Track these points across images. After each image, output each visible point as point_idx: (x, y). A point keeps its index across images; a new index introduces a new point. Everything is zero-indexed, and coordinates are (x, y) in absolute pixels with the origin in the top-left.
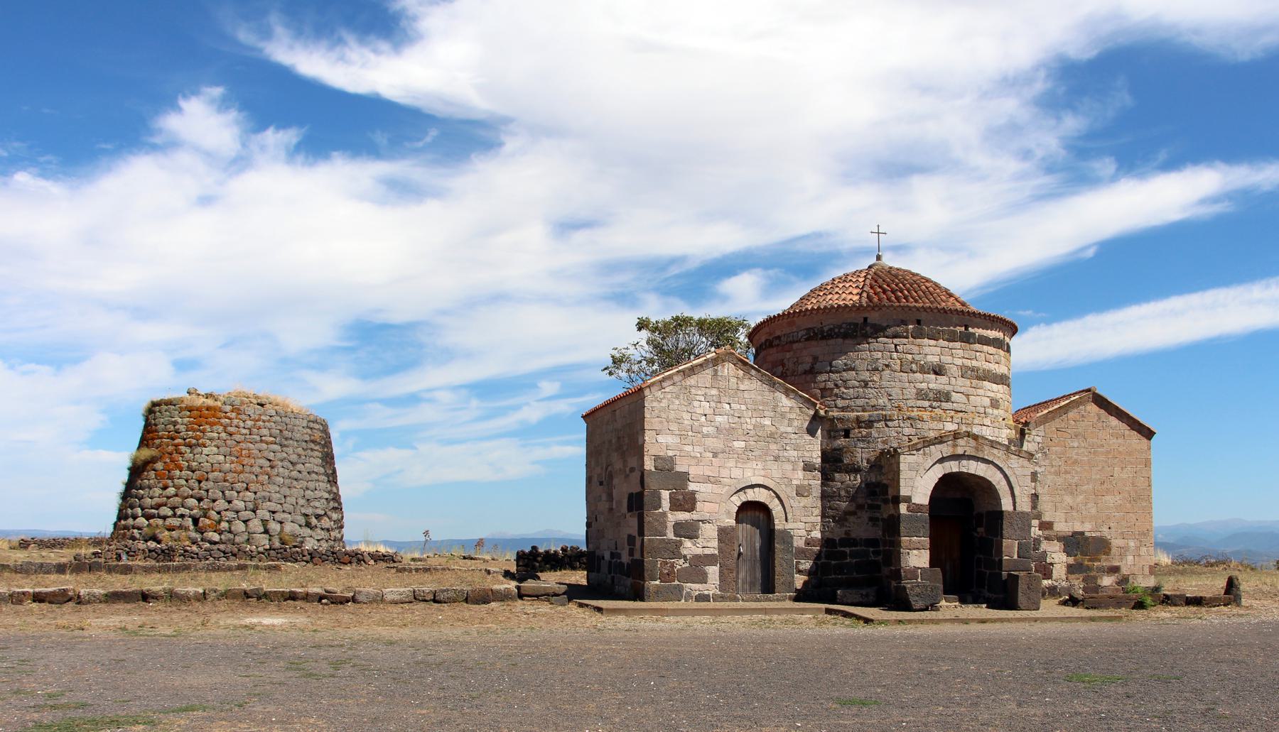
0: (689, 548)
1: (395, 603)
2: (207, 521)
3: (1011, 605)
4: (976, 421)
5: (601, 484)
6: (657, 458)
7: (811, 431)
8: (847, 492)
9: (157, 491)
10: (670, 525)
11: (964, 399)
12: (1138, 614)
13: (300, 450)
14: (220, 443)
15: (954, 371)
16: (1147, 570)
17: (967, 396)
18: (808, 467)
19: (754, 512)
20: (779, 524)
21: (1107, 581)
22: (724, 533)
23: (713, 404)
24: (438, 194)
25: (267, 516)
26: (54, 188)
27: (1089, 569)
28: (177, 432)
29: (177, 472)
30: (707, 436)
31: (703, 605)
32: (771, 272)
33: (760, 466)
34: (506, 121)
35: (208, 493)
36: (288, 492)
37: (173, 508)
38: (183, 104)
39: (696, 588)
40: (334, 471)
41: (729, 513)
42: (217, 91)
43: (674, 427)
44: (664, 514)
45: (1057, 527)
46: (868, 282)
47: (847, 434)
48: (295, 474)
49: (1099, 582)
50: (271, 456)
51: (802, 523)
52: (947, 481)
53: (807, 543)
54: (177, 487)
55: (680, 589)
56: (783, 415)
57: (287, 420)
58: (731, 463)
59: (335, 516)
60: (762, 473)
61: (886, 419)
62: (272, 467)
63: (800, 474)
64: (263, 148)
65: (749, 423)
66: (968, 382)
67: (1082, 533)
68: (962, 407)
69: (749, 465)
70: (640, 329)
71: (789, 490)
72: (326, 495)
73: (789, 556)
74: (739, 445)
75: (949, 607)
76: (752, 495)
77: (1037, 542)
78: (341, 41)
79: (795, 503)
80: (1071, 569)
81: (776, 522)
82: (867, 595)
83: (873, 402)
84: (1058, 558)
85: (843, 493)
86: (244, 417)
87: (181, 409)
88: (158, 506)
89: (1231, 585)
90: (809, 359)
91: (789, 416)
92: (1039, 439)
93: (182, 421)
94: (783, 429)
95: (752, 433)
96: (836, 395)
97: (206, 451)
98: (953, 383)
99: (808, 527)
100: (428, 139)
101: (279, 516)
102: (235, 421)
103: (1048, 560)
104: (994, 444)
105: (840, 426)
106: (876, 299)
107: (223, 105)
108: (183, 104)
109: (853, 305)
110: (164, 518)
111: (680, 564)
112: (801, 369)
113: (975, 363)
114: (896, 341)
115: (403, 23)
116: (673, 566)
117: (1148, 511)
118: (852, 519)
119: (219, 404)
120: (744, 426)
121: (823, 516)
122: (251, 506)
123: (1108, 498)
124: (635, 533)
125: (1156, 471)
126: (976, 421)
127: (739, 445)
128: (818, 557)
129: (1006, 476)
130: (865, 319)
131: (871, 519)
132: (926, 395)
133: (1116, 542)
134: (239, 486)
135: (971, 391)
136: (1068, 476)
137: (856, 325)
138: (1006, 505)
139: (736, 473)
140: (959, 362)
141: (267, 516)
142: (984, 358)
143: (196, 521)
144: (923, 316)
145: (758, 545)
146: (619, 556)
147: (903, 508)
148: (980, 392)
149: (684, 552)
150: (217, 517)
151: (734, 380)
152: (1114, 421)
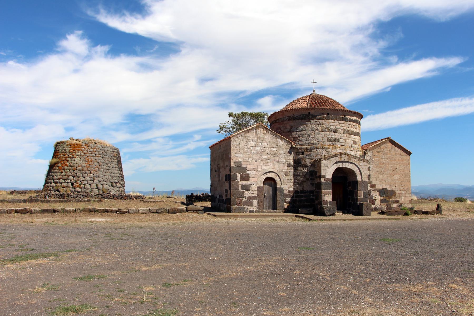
0: (247, 194)
1: (143, 213)
2: (77, 184)
3: (360, 214)
4: (348, 149)
5: (216, 171)
6: (235, 162)
8: (303, 174)
9: (59, 174)
10: (240, 186)
11: (344, 141)
12: (406, 217)
13: (109, 159)
14: (81, 157)
16: (409, 202)
17: (345, 140)
18: (289, 165)
19: (270, 181)
20: (279, 185)
21: (395, 206)
22: (259, 189)
23: (255, 143)
24: (158, 68)
25: (98, 183)
26: (22, 67)
27: (388, 201)
28: (66, 153)
29: (66, 167)
30: (253, 154)
31: (252, 214)
32: (276, 96)
33: (272, 165)
34: (182, 43)
35: (77, 174)
36: (105, 174)
37: (65, 180)
38: (68, 37)
39: (249, 208)
40: (121, 167)
41: (261, 181)
42: (80, 32)
43: (242, 151)
44: (238, 182)
45: (377, 187)
46: (310, 100)
47: (303, 154)
48: (107, 168)
49: (392, 206)
50: (99, 161)
51: (287, 185)
52: (338, 171)
53: (289, 192)
54: (66, 172)
55: (244, 208)
56: (280, 147)
57: (105, 149)
58: (262, 164)
59: (122, 183)
60: (273, 167)
61: (317, 148)
62: (99, 165)
63: (286, 168)
64: (96, 52)
65: (268, 150)
66: (345, 135)
67: (386, 189)
69: (268, 164)
70: (229, 116)
71: (282, 173)
72: (119, 175)
74: (264, 157)
75: (339, 215)
76: (269, 175)
77: (370, 192)
78: (124, 15)
79: (284, 178)
80: (382, 201)
81: (278, 185)
82: (310, 211)
83: (312, 142)
84: (377, 197)
85: (301, 174)
86: (89, 147)
87: (67, 145)
88: (59, 179)
89: (438, 207)
90: (289, 127)
91: (282, 147)
92: (370, 155)
93: (68, 149)
94: (280, 152)
95: (269, 153)
96: (299, 140)
97: (76, 159)
98: (341, 135)
99: (289, 186)
100: (155, 49)
101: (102, 183)
102: (87, 149)
104: (354, 157)
105: (300, 151)
106: (313, 106)
107: (82, 37)
108: (68, 37)
109: (305, 108)
110: (61, 183)
112: (286, 130)
113: (348, 128)
114: (320, 121)
115: (146, 8)
116: (241, 200)
117: (409, 181)
118: (304, 183)
119: (81, 143)
121: (294, 182)
122: (92, 179)
123: (395, 176)
124: (228, 189)
125: (412, 167)
126: (348, 149)
127: (264, 157)
128: (292, 197)
130: (309, 113)
131: (311, 184)
132: (331, 140)
133: (398, 192)
134: (88, 172)
135: (347, 138)
136: (381, 168)
138: (359, 179)
139: (264, 167)
140: (342, 128)
141: (98, 183)
142: (351, 127)
143: (72, 184)
144: (330, 112)
145: (271, 193)
146: (222, 197)
147: (322, 180)
148: (350, 139)
149: (245, 195)
150: (80, 183)
151: (263, 135)
152: (397, 149)
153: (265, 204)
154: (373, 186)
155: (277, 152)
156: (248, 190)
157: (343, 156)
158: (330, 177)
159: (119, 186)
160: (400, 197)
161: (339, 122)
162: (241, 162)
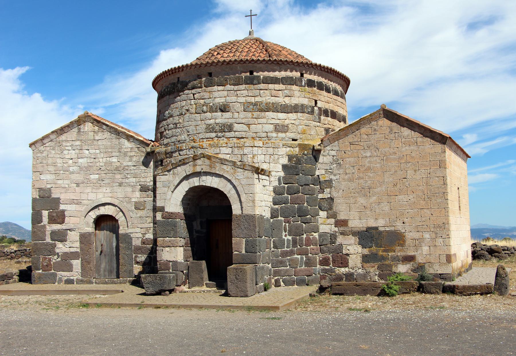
0: (61, 248)
7: (146, 164)
10: (48, 234)
11: (245, 128)
15: (239, 107)
18: (144, 189)
20: (122, 230)
22: (84, 238)
23: (77, 151)
27: (383, 258)
30: (73, 173)
31: (70, 287)
39: (64, 275)
43: (51, 169)
44: (44, 226)
45: (351, 224)
53: (143, 243)
55: (55, 275)
56: (125, 154)
60: (110, 195)
63: (138, 194)
65: (102, 161)
66: (249, 115)
67: (376, 228)
68: (244, 134)
69: (100, 190)
71: (129, 206)
73: (129, 252)
80: (365, 259)
81: (121, 228)
83: (179, 138)
84: (354, 250)
91: (129, 154)
92: (333, 153)
94: (125, 164)
95: (103, 168)
98: (237, 117)
99: (143, 231)
103: (344, 252)
104: (223, 162)
111: (55, 259)
113: (258, 99)
114: (194, 91)
116: (50, 260)
120: (98, 164)
123: (400, 197)
129: (234, 187)
133: (410, 235)
136: (361, 181)
137: (174, 84)
138: (236, 210)
139: (92, 196)
140: (242, 100)
144: (212, 69)
149: (57, 251)
151: (92, 134)
152: (406, 131)
153: (103, 266)
154: (341, 223)
155: (118, 164)
156: (63, 239)
157: (199, 162)
158: (180, 210)
160: (417, 247)
161: (236, 88)
162: (50, 189)
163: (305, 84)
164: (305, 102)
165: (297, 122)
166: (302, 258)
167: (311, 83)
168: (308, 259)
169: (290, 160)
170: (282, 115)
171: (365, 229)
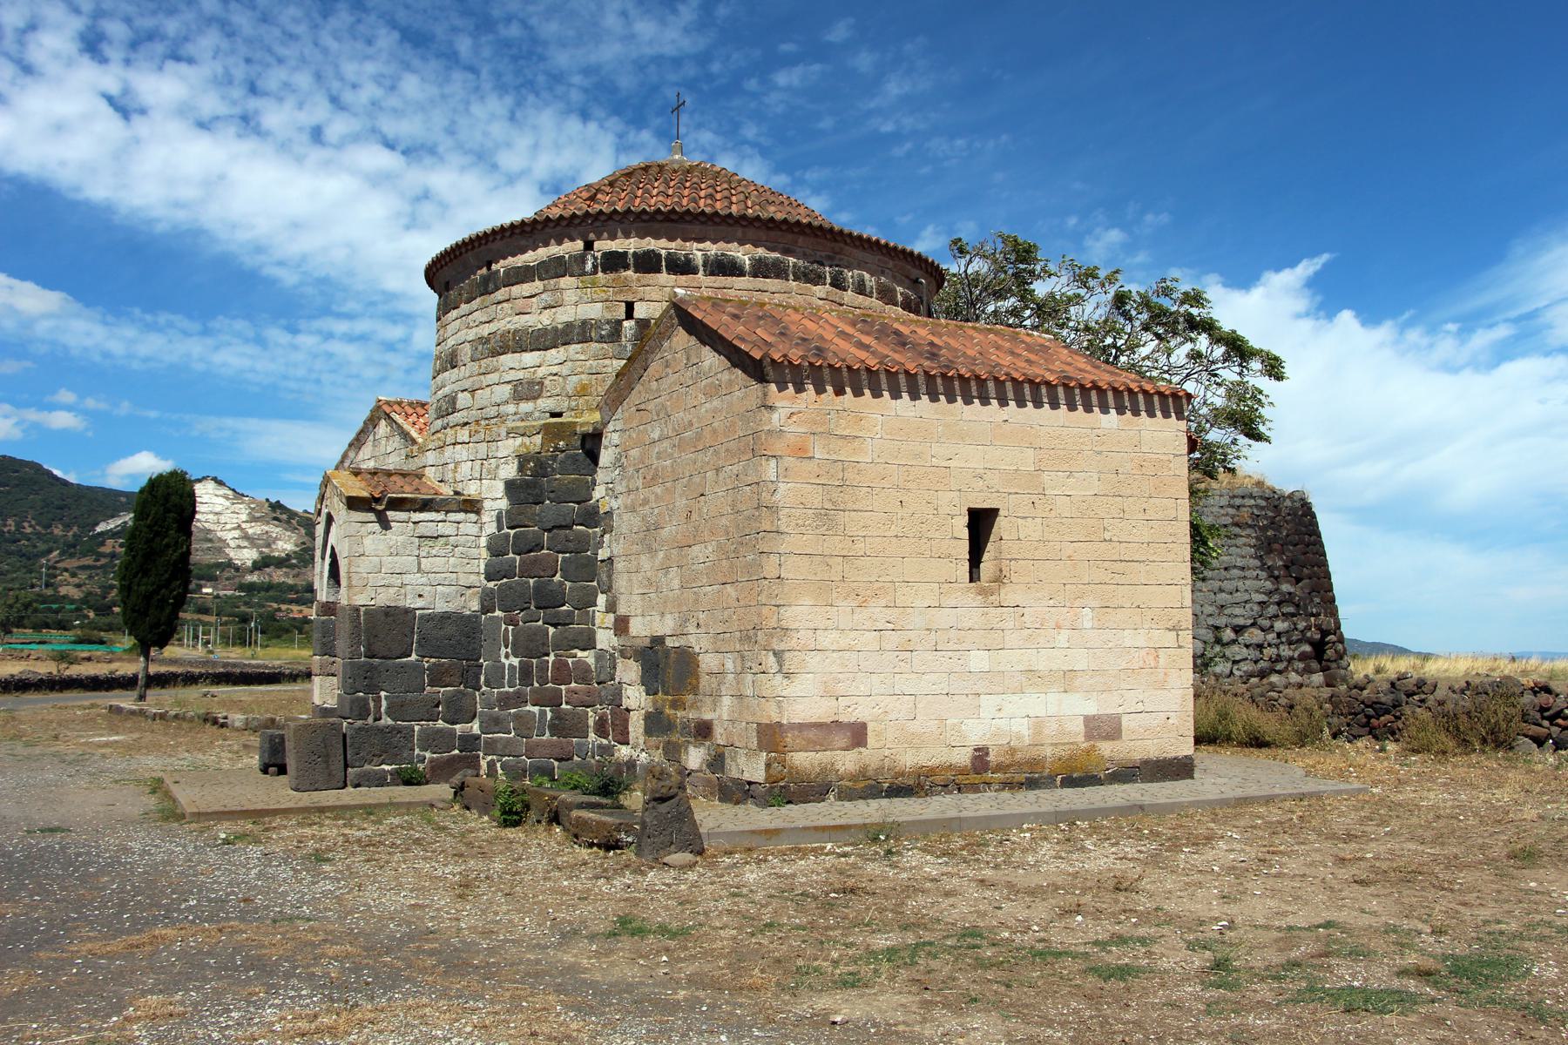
113: (492, 327)
159: (1255, 640)
163: (595, 266)
164: (594, 311)
165: (565, 370)
166: (543, 714)
167: (614, 262)
168: (558, 716)
169: (521, 469)
170: (530, 358)
171: (647, 643)
